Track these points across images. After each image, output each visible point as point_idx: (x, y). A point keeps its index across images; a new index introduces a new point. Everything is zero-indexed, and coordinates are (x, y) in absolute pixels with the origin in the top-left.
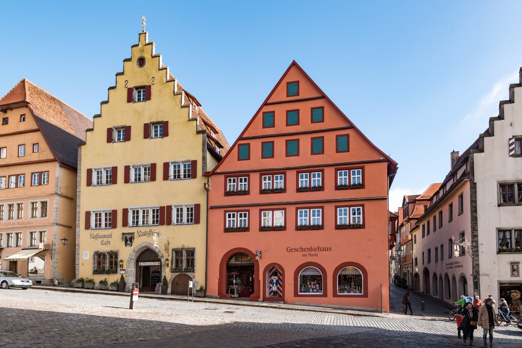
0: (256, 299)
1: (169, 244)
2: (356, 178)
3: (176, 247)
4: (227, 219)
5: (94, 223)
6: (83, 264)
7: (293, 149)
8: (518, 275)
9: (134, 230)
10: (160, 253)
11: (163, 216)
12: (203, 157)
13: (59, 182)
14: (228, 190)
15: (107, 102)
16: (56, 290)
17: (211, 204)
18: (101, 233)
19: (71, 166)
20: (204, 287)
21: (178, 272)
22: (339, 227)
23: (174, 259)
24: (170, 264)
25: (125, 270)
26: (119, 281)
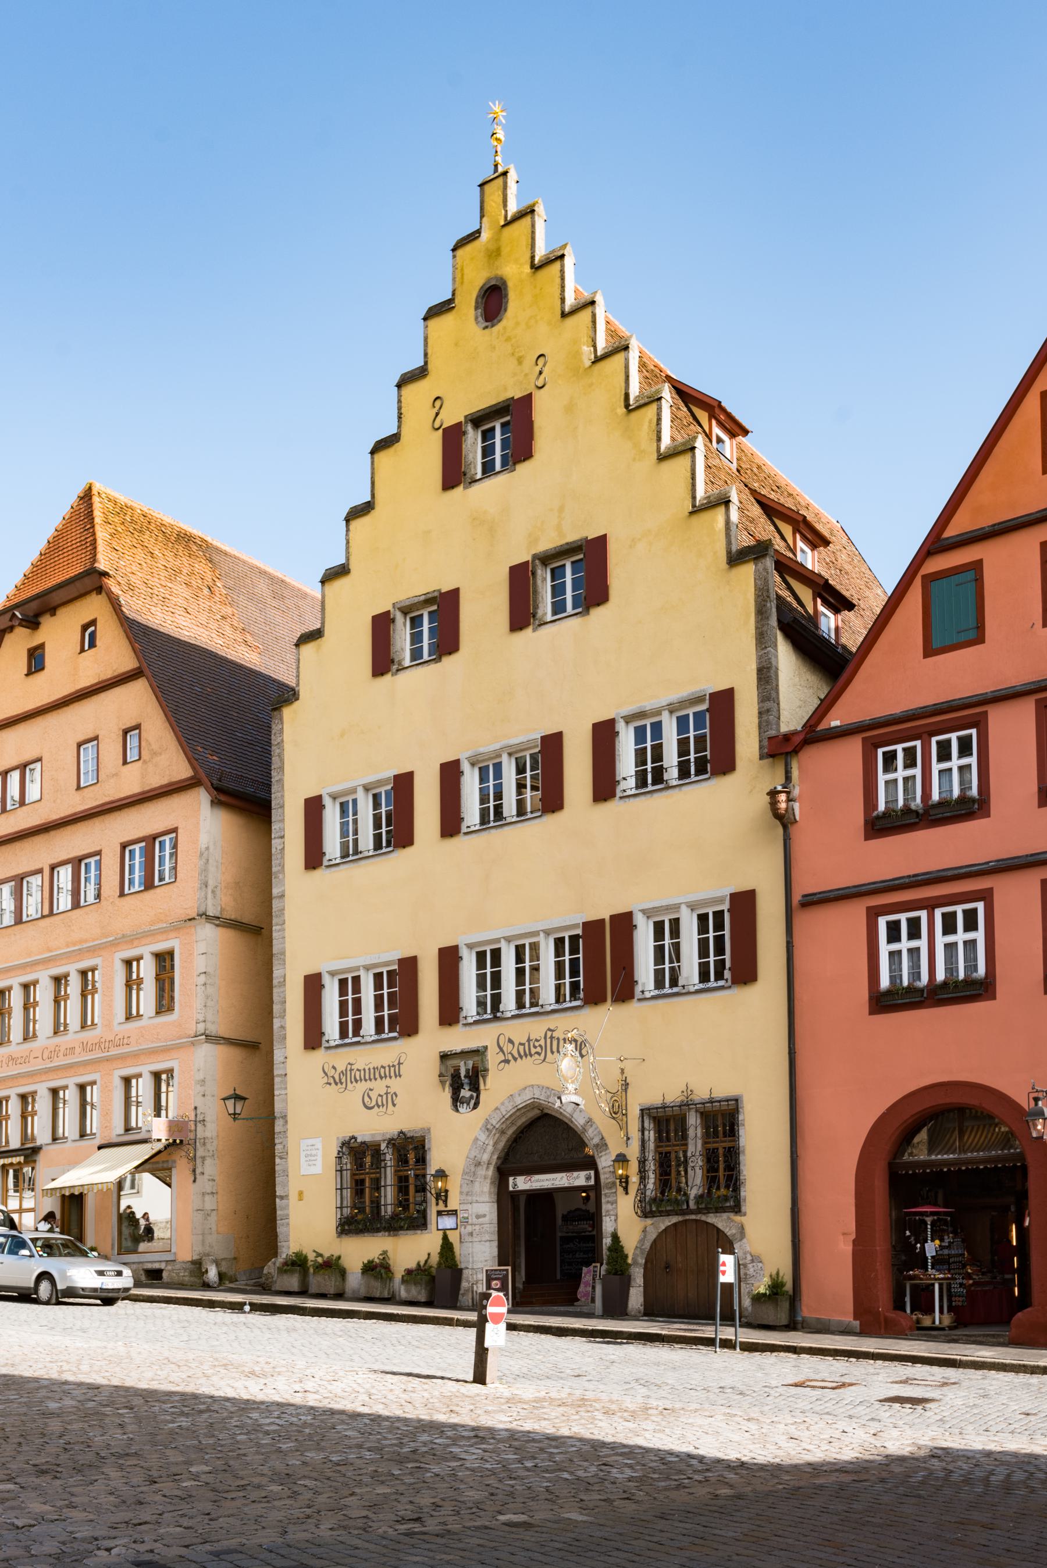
1: (626, 1085)
4: (885, 948)
5: (336, 1019)
6: (301, 1193)
9: (483, 1037)
11: (599, 962)
13: (212, 869)
14: (882, 807)
16: (211, 1304)
17: (806, 884)
18: (364, 1058)
19: (248, 797)
21: (668, 1214)
23: (650, 1156)
24: (634, 1179)
25: (454, 1213)
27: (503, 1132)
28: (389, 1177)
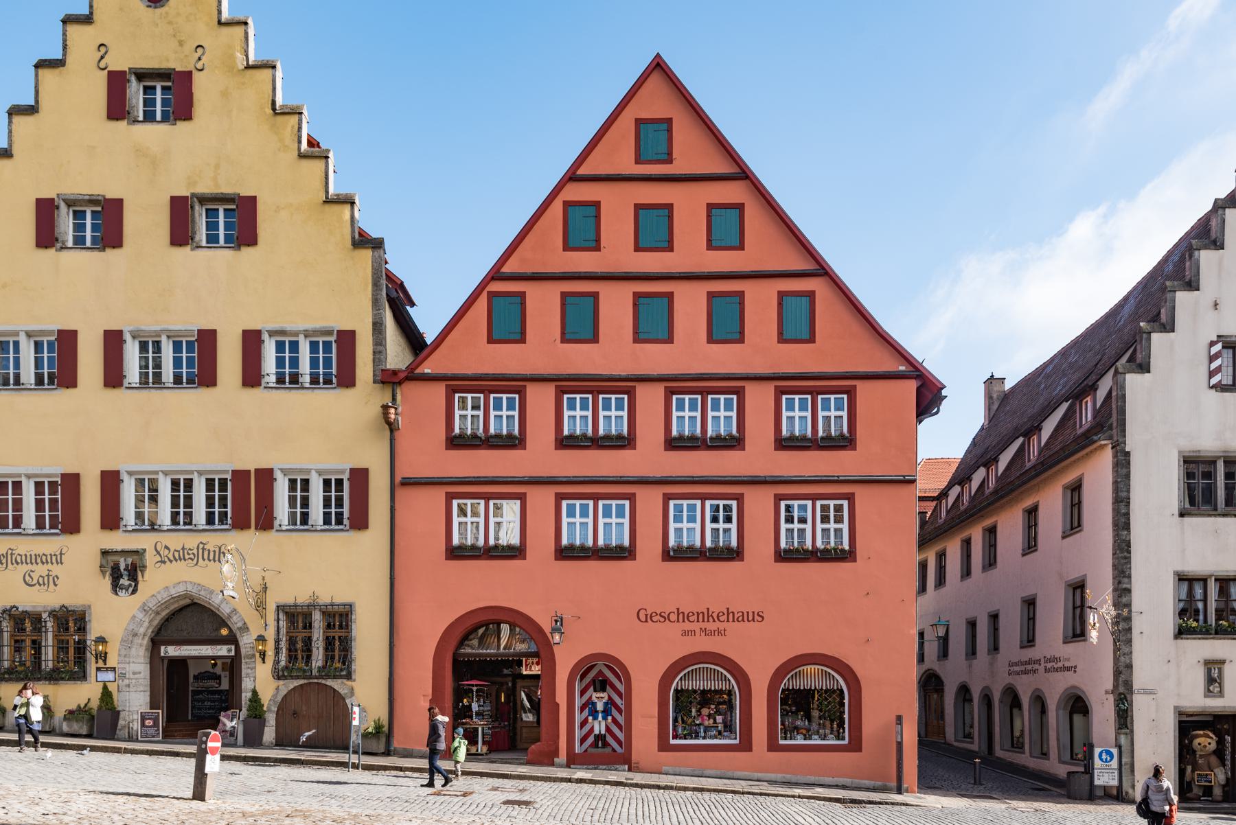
0: (548, 759)
1: (265, 588)
2: (833, 414)
3: (289, 600)
4: (456, 520)
7: (653, 322)
8: (1221, 694)
10: (235, 618)
11: (244, 500)
12: (375, 324)
14: (457, 431)
15: (32, 110)
17: (403, 472)
20: (385, 722)
21: (298, 677)
22: (784, 556)
24: (270, 653)
26: (95, 704)
27: (158, 613)
28: (49, 640)
